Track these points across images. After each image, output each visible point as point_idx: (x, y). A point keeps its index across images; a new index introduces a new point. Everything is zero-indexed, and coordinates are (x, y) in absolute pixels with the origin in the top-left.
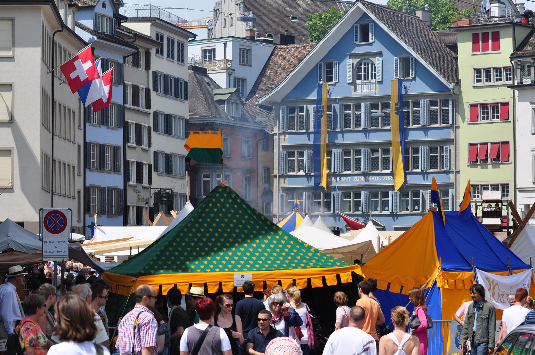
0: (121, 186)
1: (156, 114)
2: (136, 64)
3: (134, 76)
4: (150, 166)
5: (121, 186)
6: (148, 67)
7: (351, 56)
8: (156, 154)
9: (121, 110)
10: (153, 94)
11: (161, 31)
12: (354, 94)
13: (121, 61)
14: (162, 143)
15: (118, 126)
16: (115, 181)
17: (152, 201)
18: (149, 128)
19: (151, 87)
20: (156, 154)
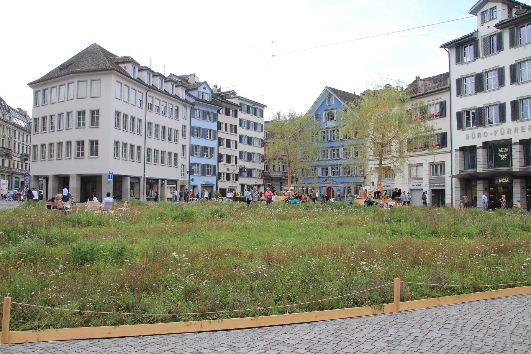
0: (215, 164)
1: (241, 137)
2: (227, 113)
3: (222, 118)
4: (236, 157)
5: (215, 164)
6: (236, 116)
7: (325, 110)
8: (241, 153)
9: (215, 133)
10: (239, 128)
11: (241, 102)
12: (326, 127)
13: (216, 112)
14: (243, 147)
15: (214, 139)
16: (213, 162)
17: (237, 172)
18: (236, 142)
19: (238, 124)
20: (241, 153)
